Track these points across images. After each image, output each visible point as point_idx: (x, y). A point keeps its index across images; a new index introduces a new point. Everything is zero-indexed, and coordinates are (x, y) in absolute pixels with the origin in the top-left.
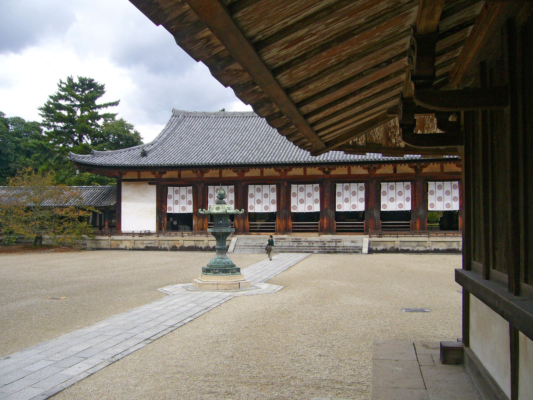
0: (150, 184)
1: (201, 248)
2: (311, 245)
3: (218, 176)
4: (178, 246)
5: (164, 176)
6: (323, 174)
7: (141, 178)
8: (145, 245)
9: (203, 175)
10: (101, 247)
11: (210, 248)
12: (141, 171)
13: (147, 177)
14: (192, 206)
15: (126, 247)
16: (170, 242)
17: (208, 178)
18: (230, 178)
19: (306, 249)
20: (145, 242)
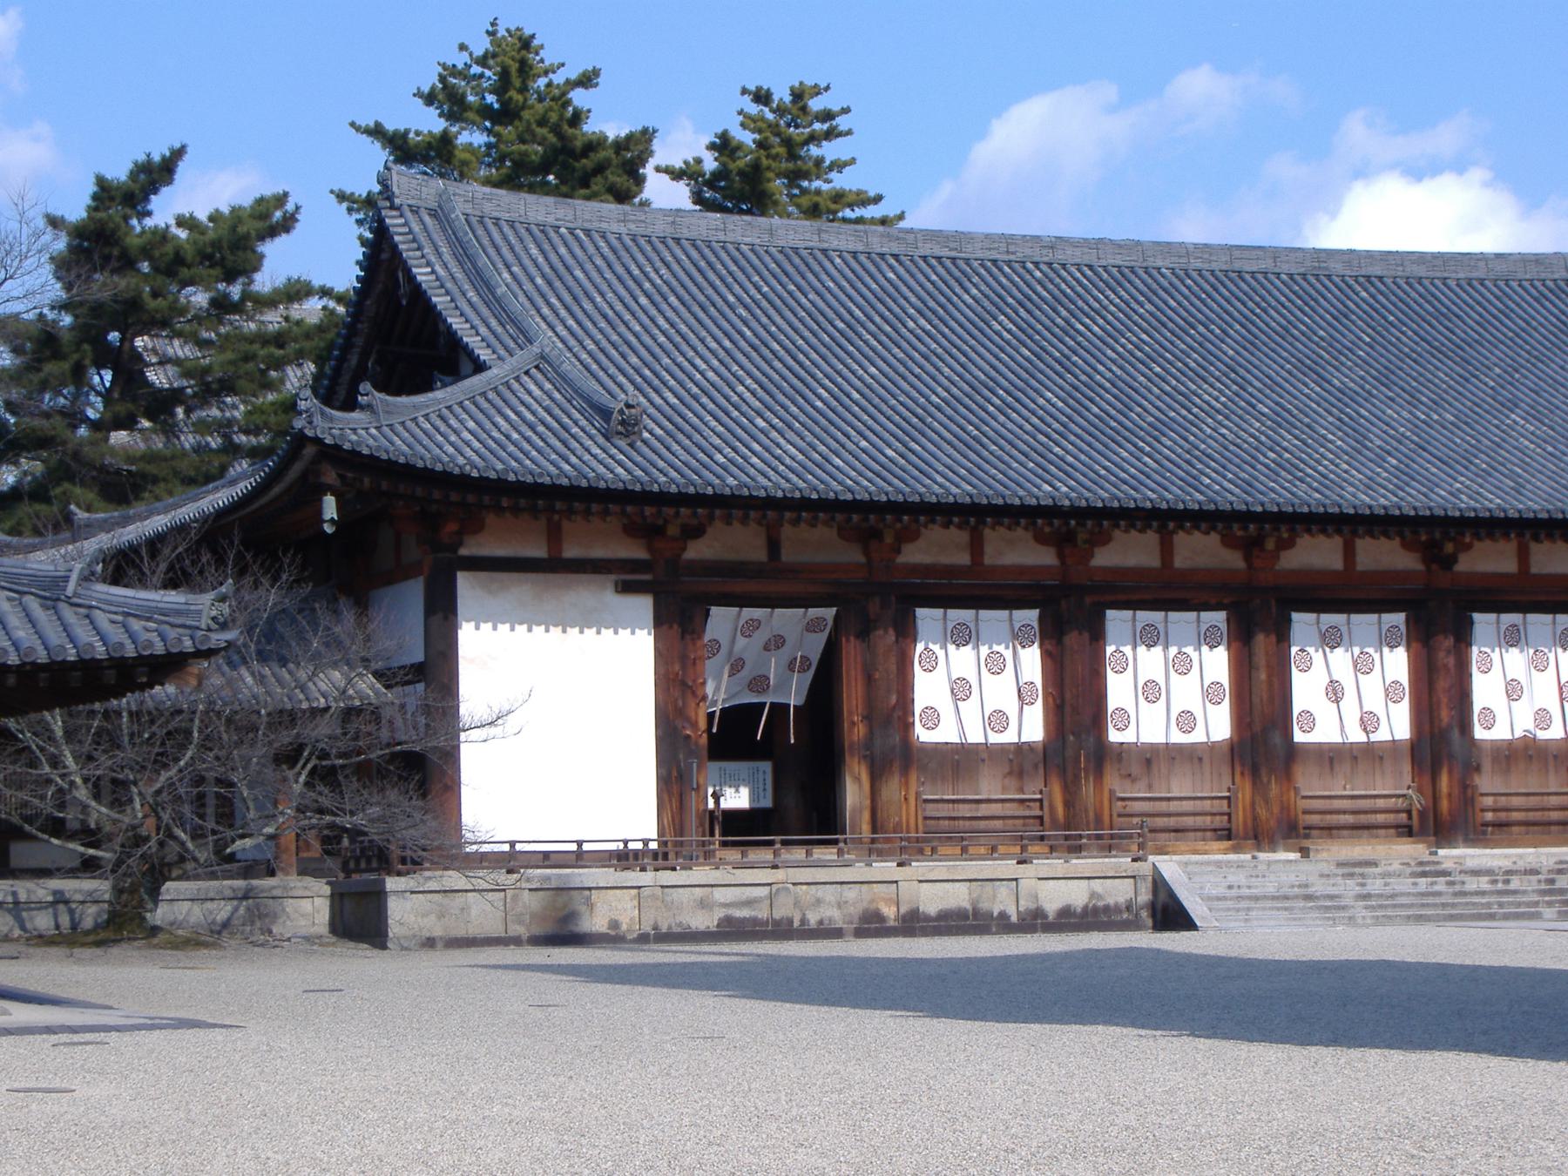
0: (626, 588)
1: (1003, 916)
2: (1500, 886)
3: (964, 559)
4: (889, 912)
5: (697, 551)
6: (1420, 567)
7: (571, 552)
8: (719, 913)
9: (899, 552)
10: (473, 931)
11: (1045, 916)
12: (570, 512)
13: (598, 552)
14: (1112, 704)
15: (615, 924)
16: (851, 893)
17: (915, 569)
18: (1021, 570)
19: (1501, 905)
20: (720, 895)
